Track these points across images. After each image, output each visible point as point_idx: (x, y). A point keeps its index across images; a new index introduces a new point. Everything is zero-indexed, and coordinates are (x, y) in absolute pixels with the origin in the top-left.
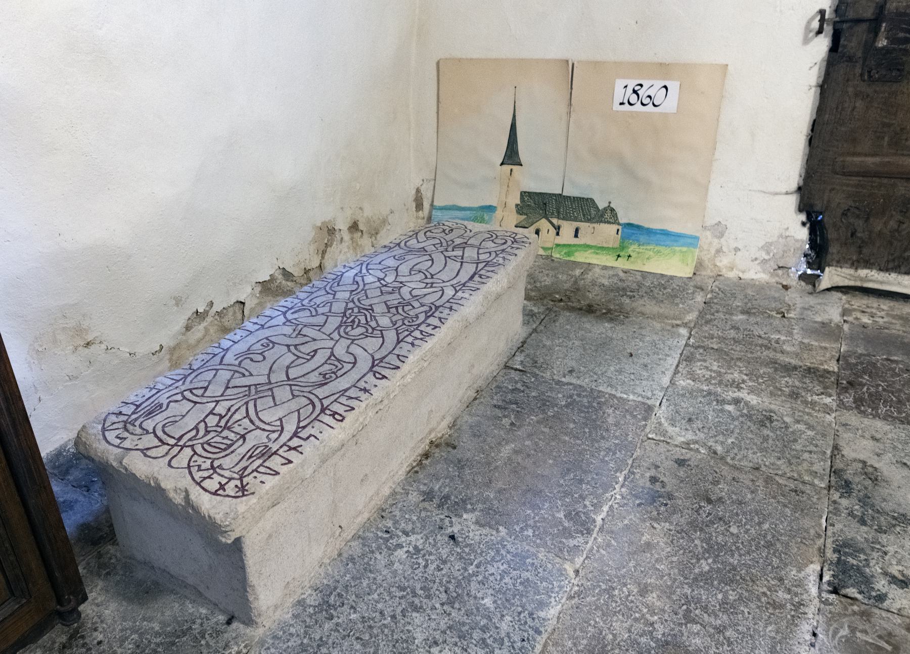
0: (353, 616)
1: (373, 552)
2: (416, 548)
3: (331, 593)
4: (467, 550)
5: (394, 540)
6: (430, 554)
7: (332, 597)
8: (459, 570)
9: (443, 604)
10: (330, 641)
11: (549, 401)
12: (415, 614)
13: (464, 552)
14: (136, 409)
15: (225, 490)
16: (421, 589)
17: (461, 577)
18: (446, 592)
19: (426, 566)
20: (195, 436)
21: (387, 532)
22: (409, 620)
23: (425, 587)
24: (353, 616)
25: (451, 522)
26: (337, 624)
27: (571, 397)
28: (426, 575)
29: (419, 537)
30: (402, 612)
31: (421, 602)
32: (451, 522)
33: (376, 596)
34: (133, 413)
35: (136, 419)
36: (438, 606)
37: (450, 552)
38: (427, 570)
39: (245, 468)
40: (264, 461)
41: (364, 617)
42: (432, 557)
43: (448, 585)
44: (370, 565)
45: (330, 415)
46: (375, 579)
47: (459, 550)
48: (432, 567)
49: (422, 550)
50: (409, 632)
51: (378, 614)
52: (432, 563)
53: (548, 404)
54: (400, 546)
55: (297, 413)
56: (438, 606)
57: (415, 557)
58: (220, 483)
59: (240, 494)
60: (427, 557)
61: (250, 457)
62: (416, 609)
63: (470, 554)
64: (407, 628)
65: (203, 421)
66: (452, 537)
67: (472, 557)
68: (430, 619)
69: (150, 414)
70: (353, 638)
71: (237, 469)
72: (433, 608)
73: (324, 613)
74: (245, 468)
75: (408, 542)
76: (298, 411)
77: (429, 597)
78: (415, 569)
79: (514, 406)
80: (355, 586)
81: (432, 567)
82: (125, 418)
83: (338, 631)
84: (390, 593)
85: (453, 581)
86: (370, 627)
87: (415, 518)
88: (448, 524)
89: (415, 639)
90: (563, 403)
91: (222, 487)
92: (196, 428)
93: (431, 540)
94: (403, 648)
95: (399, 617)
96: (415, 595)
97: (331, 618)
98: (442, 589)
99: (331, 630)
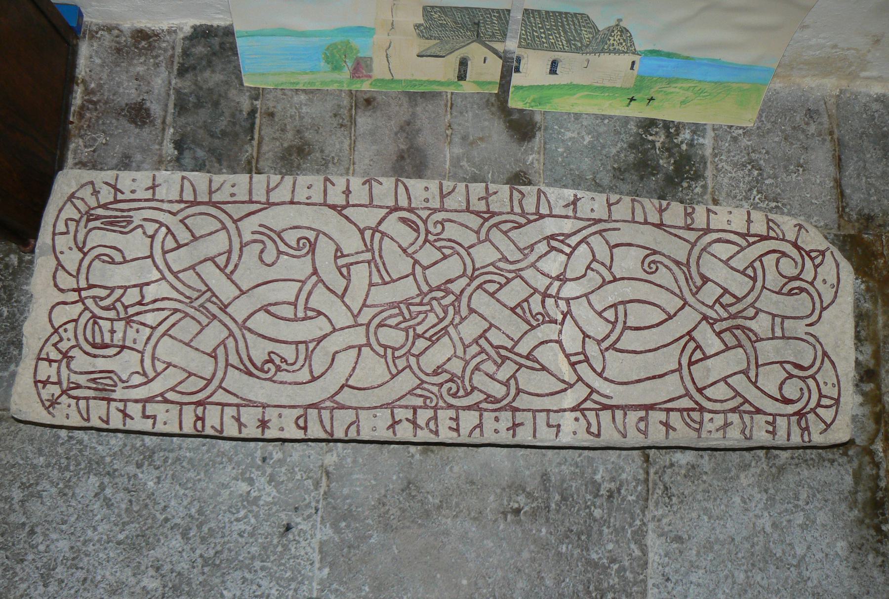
0: (151, 484)
1: (230, 460)
2: (257, 498)
3: (165, 450)
4: (280, 549)
5: (256, 473)
6: (256, 517)
7: (162, 454)
8: (249, 553)
9: (201, 556)
10: (117, 480)
11: (589, 536)
12: (179, 537)
13: (276, 546)
14: (111, 203)
15: (44, 388)
16: (209, 529)
17: (240, 558)
18: (216, 553)
19: (238, 520)
20: (102, 299)
21: (264, 460)
22: (170, 536)
23: (214, 531)
24: (151, 484)
25: (309, 516)
26: (135, 476)
27: (613, 561)
28: (228, 525)
29: (274, 493)
30: (176, 524)
31: (195, 536)
32: (309, 516)
33: (182, 492)
34: (104, 206)
35: (98, 218)
36: (198, 552)
37: (269, 534)
38: (235, 523)
39: (78, 387)
40: (94, 398)
41: (153, 494)
42: (253, 521)
43: (226, 551)
44: (213, 466)
45: (197, 416)
46: (200, 480)
47: (275, 541)
48: (241, 526)
49: (258, 506)
50: (157, 542)
51: (163, 504)
52: (245, 523)
53: (583, 538)
54: (251, 481)
55: (187, 375)
56: (198, 552)
57: (245, 503)
58: (49, 377)
59: (47, 404)
60: (250, 515)
61: (94, 380)
62: (185, 535)
63: (275, 553)
64: (161, 537)
65: (126, 288)
66: (288, 528)
67: (272, 558)
68: (180, 552)
69: (111, 224)
70: (130, 498)
71: (74, 378)
72: (193, 550)
73: (142, 457)
74: (78, 387)
75: (261, 487)
76: (190, 374)
77: (203, 540)
78: (230, 512)
79: (557, 497)
80: (183, 467)
81: (241, 526)
82: (93, 203)
83: (129, 481)
84: (191, 503)
85: (233, 553)
86: (146, 505)
87: (298, 477)
88: (307, 513)
89: (154, 549)
90: (594, 556)
91: (45, 383)
92: (112, 289)
93: (274, 509)
94: (139, 544)
95: (168, 525)
96: (199, 527)
97: (139, 466)
98: (219, 548)
99: (128, 474)
